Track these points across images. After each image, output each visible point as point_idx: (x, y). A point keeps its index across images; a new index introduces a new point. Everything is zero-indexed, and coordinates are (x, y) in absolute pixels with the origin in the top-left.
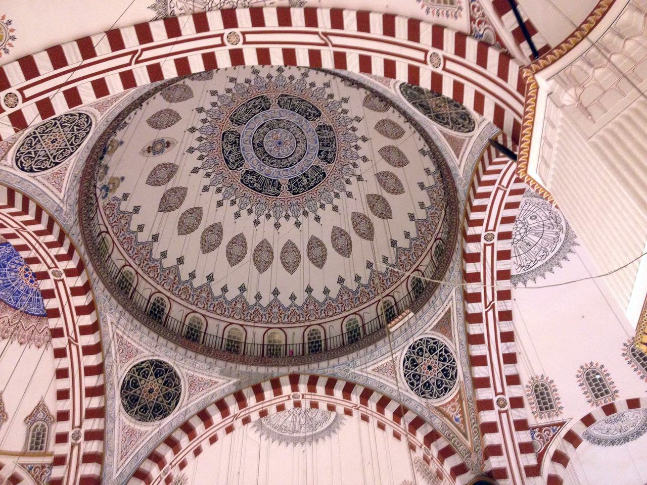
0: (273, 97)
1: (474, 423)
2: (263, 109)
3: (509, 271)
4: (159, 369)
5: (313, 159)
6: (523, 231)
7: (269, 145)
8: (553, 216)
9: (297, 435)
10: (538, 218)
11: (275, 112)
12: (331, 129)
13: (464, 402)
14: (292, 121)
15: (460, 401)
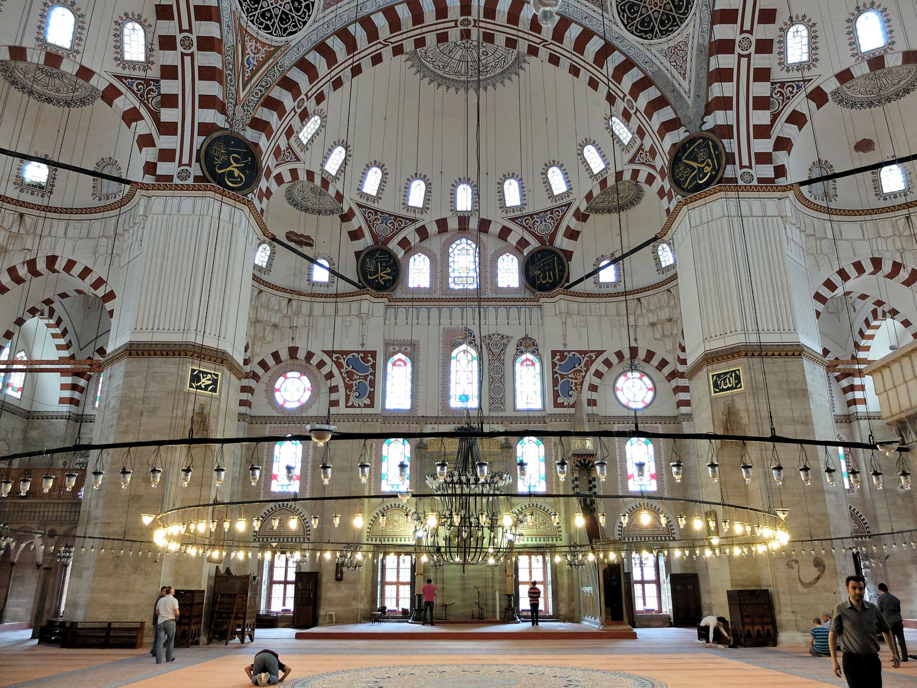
1: (262, 86)
3: (424, 45)
8: (489, 69)
10: (484, 57)
13: (271, 61)
15: (269, 55)
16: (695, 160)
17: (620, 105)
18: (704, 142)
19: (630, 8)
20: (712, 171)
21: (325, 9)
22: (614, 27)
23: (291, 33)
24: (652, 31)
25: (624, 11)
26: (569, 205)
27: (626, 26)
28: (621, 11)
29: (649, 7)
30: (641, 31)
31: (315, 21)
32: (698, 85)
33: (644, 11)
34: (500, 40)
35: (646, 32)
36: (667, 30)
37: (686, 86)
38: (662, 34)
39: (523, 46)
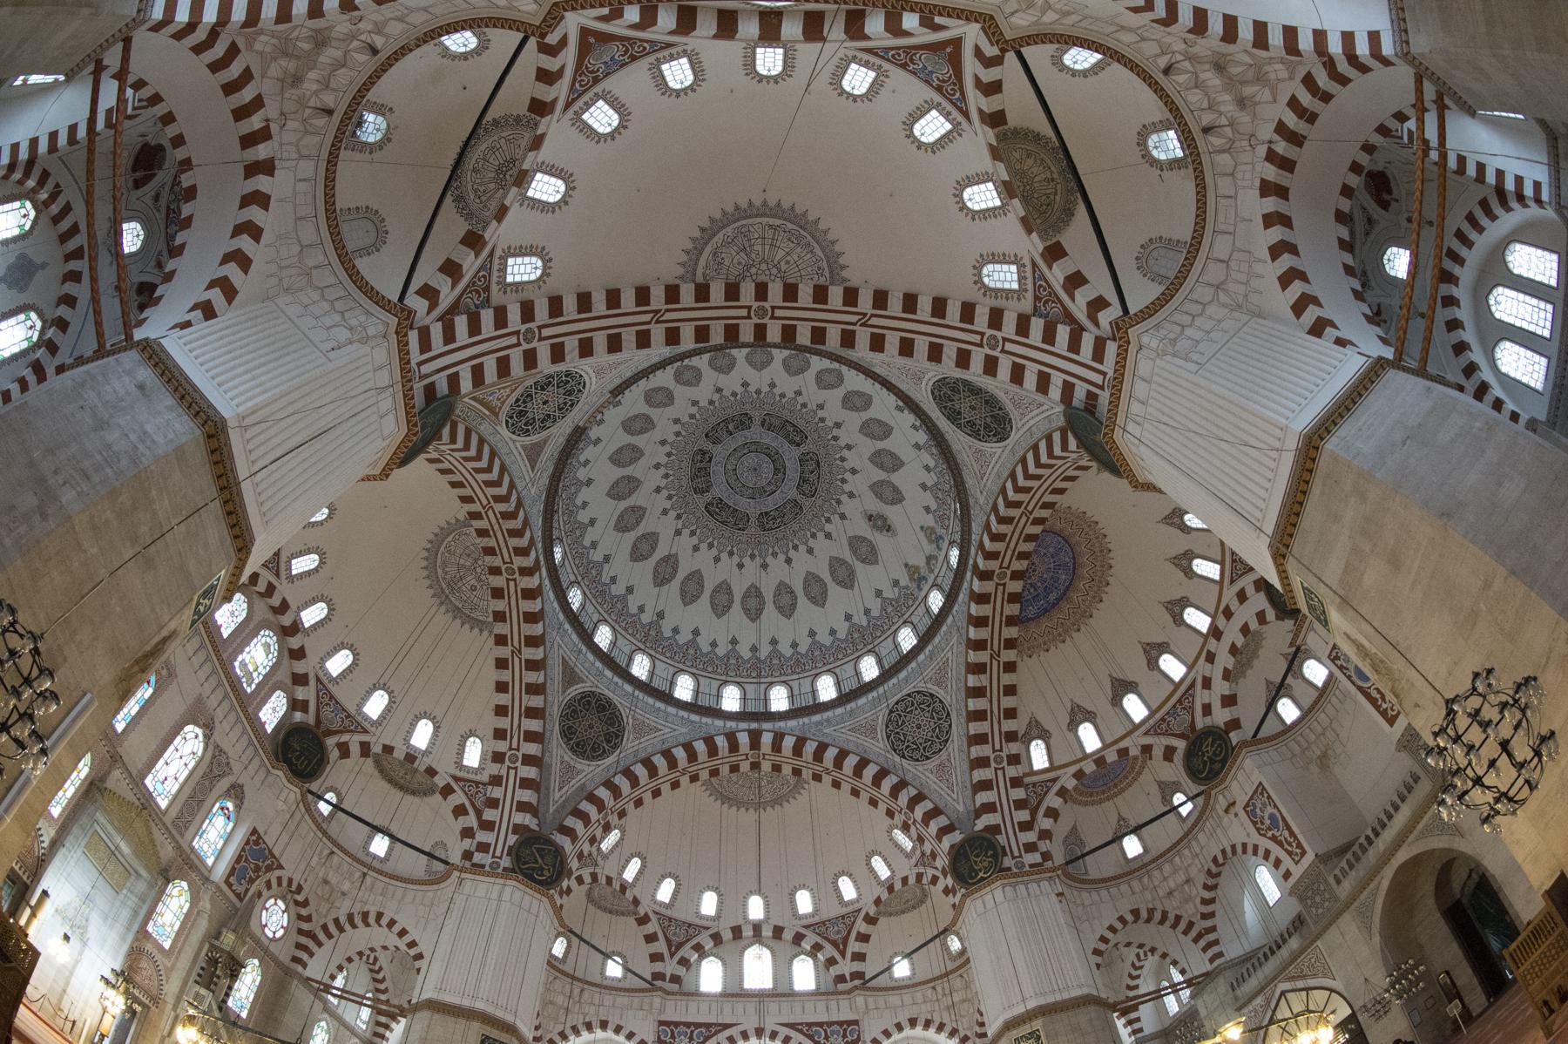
0: (753, 529)
2: (766, 513)
4: (953, 416)
5: (719, 452)
6: (479, 570)
7: (767, 468)
9: (771, 221)
11: (753, 508)
12: (695, 490)
14: (738, 497)
17: (502, 746)
21: (522, 446)
22: (556, 708)
23: (507, 422)
26: (366, 731)
28: (569, 705)
31: (514, 442)
32: (563, 805)
34: (500, 605)
37: (557, 796)
39: (502, 629)
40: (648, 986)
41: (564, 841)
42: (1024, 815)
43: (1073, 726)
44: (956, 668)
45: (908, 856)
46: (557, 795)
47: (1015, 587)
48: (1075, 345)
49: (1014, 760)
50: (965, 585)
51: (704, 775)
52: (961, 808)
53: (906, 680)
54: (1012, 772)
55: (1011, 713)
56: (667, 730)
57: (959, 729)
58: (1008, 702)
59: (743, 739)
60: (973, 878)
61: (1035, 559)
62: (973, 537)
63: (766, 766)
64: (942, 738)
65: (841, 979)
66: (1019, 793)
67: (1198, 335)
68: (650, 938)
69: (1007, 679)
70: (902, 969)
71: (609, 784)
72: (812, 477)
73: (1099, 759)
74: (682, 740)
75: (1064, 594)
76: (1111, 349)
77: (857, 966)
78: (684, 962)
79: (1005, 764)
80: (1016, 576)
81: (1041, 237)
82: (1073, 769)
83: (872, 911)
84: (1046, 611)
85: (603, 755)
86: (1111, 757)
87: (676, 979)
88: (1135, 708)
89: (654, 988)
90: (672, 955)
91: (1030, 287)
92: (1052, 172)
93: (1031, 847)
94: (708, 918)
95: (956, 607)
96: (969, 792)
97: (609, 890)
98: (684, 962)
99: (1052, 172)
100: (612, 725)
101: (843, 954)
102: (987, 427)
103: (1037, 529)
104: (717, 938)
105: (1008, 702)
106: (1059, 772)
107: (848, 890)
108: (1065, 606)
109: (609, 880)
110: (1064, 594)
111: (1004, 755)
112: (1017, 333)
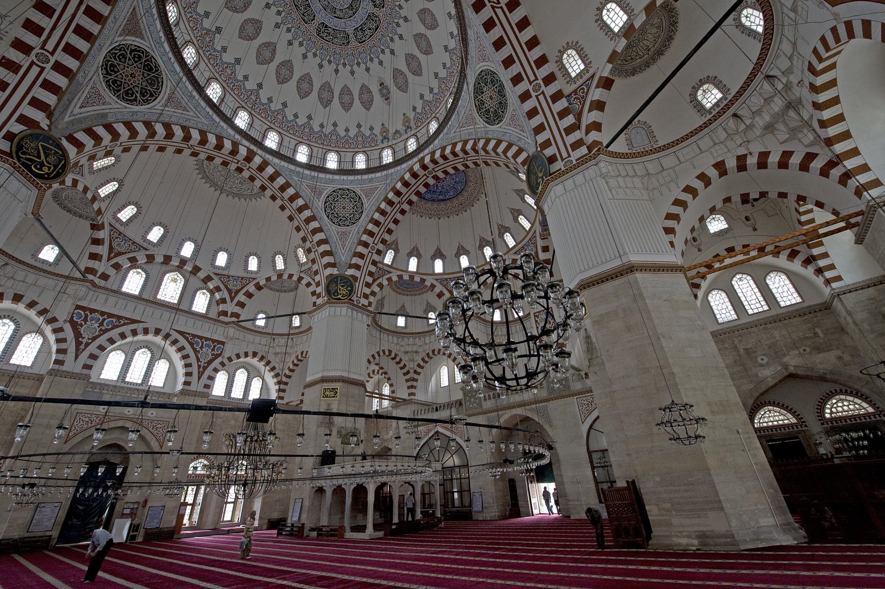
0: (312, 27)
2: (326, 26)
4: (478, 91)
11: (322, 17)
16: (46, 156)
18: (60, 155)
19: (121, 55)
20: (47, 173)
22: (108, 43)
24: (108, 73)
25: (120, 50)
27: (109, 52)
28: (121, 48)
29: (125, 71)
30: (106, 65)
32: (80, 121)
33: (122, 67)
35: (106, 69)
36: (110, 86)
38: (106, 82)
40: (82, 277)
41: (72, 150)
42: (369, 280)
43: (410, 255)
44: (378, 195)
45: (301, 265)
46: (77, 111)
47: (431, 181)
48: (569, 130)
49: (379, 252)
50: (410, 162)
51: (202, 156)
52: (343, 259)
53: (352, 182)
54: (376, 257)
55: (390, 232)
56: (191, 114)
57: (363, 222)
58: (392, 226)
59: (243, 151)
60: (334, 295)
61: (448, 178)
62: (432, 146)
63: (246, 174)
64: (353, 221)
65: (224, 313)
66: (373, 269)
67: (622, 185)
68: (96, 242)
69: (399, 216)
70: (261, 323)
71: (128, 125)
72: (368, 32)
73: (412, 276)
74: (200, 126)
75: (445, 200)
76: (584, 150)
77: (237, 310)
78: (117, 266)
79: (374, 251)
80: (436, 178)
81: (611, 70)
82: (399, 273)
83: (262, 282)
84: (434, 200)
85: (131, 102)
86: (417, 279)
87: (105, 277)
88: (439, 266)
89: (85, 280)
90: (109, 259)
91: (579, 83)
92: (654, 46)
93: (366, 296)
94: (150, 242)
95: (399, 168)
96: (351, 254)
97: (81, 195)
98: (117, 266)
99: (654, 46)
100: (151, 85)
101: (232, 299)
102: (488, 111)
103: (462, 168)
104: (151, 258)
105: (392, 226)
106: (391, 270)
107: (253, 264)
108: (442, 204)
109: (86, 189)
110: (445, 200)
111: (376, 247)
112: (551, 97)
